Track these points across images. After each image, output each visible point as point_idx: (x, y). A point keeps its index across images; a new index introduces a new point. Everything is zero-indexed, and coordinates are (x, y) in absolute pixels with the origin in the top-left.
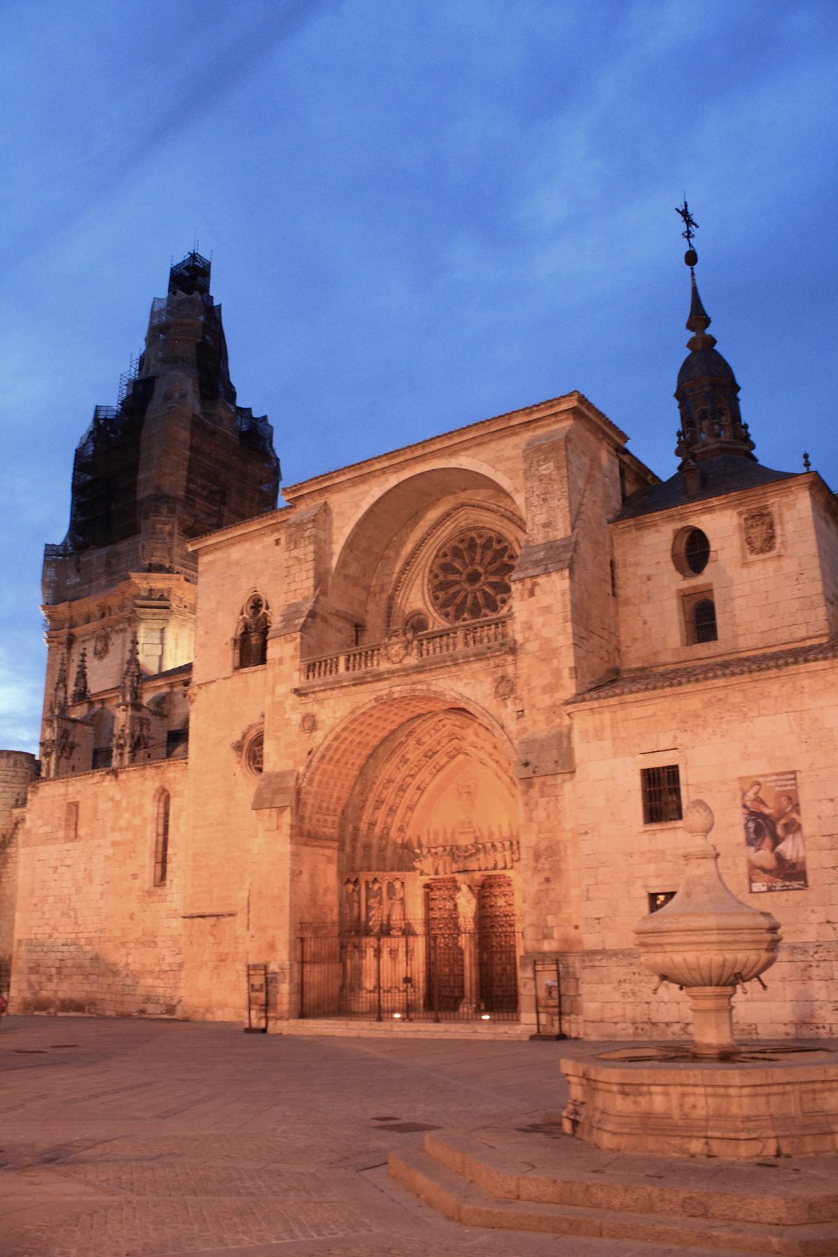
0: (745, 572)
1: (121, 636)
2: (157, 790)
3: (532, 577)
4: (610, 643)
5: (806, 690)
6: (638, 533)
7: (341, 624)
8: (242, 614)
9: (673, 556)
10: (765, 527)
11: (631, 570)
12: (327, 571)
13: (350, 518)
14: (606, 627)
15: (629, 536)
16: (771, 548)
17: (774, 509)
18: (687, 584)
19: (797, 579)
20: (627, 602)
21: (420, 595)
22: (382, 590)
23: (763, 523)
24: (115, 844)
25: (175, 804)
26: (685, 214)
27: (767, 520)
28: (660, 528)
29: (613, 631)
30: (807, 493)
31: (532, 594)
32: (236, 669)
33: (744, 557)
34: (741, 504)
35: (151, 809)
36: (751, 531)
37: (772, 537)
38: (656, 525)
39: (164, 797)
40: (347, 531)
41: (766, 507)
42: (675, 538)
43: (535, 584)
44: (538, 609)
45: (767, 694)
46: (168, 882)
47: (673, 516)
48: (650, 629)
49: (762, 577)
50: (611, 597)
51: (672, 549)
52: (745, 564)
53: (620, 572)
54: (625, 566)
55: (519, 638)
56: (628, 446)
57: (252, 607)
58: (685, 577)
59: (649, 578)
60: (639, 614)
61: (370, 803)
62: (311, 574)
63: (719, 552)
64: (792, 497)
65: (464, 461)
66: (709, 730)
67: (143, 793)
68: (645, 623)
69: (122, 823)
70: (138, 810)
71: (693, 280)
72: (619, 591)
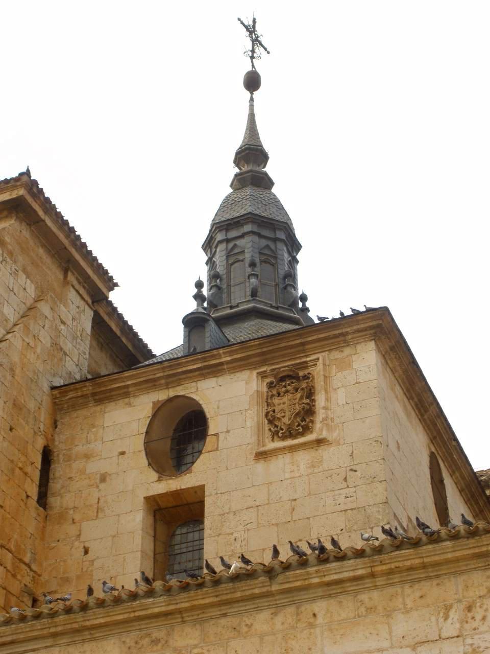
0: (260, 466)
4: (14, 576)
5: (320, 620)
6: (98, 408)
9: (147, 444)
10: (298, 395)
11: (77, 465)
14: (13, 549)
15: (84, 412)
16: (307, 429)
17: (317, 371)
19: (345, 479)
20: (62, 517)
23: (296, 390)
26: (251, 30)
27: (304, 385)
28: (132, 400)
29: (27, 559)
30: (372, 345)
33: (260, 442)
34: (264, 363)
36: (276, 401)
37: (309, 412)
38: (126, 395)
41: (304, 366)
42: (154, 416)
45: (245, 629)
47: (155, 380)
48: (93, 561)
49: (287, 476)
50: (33, 502)
51: (147, 433)
52: (262, 456)
53: (58, 469)
54: (69, 458)
56: (113, 296)
59: (103, 479)
60: (79, 536)
63: (221, 437)
64: (347, 351)
68: (86, 552)
71: (252, 107)
72: (52, 500)
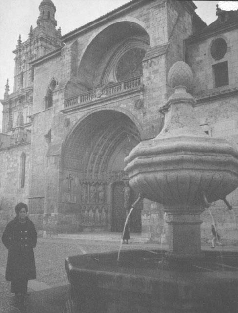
1: (26, 109)
2: (22, 154)
3: (150, 59)
7: (82, 88)
8: (49, 87)
12: (76, 67)
13: (85, 46)
18: (217, 62)
21: (112, 77)
22: (99, 75)
24: (8, 174)
25: (28, 158)
31: (150, 66)
32: (47, 108)
35: (19, 161)
39: (24, 156)
40: (84, 51)
43: (152, 61)
44: (153, 71)
46: (25, 186)
55: (145, 84)
57: (53, 85)
58: (216, 60)
61: (92, 153)
62: (70, 67)
65: (128, 18)
66: (222, 115)
67: (17, 155)
69: (11, 166)
70: (16, 161)
